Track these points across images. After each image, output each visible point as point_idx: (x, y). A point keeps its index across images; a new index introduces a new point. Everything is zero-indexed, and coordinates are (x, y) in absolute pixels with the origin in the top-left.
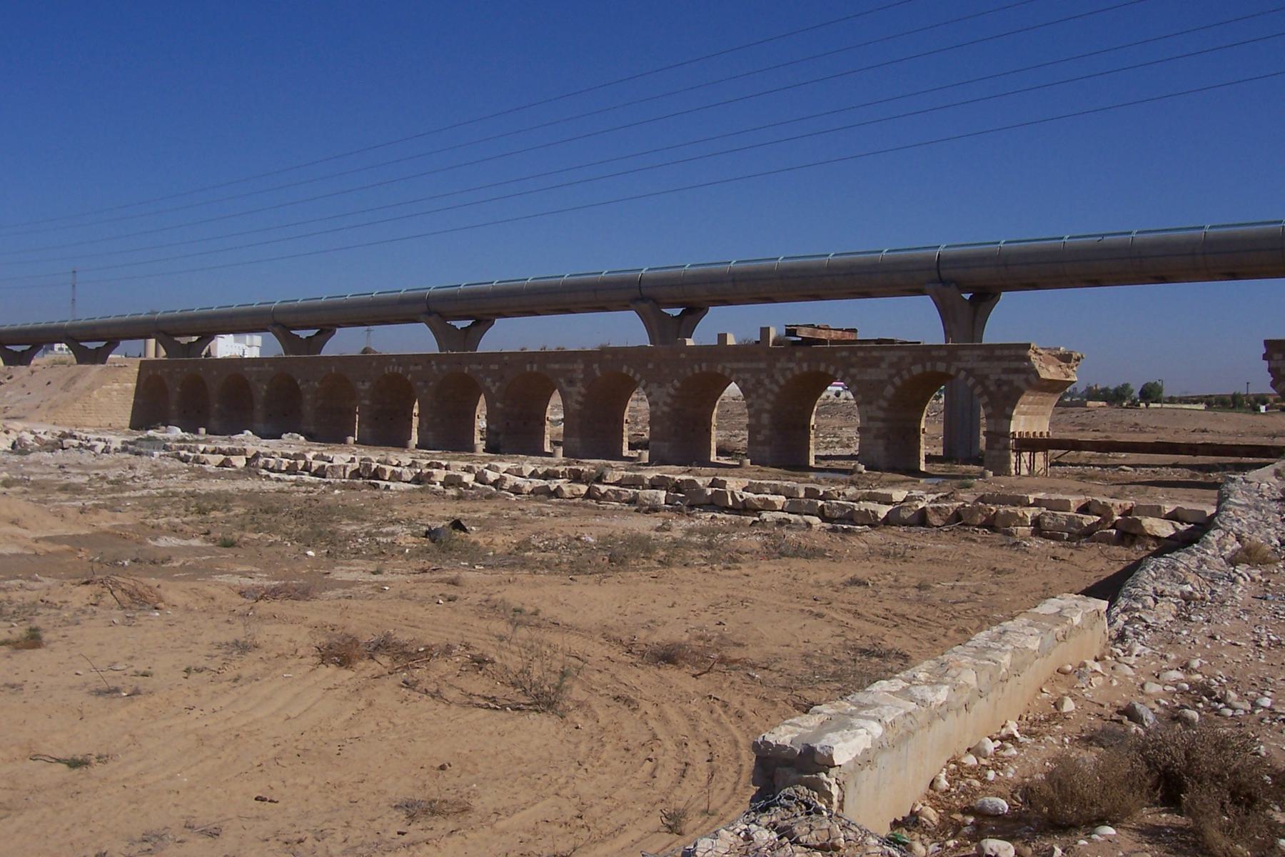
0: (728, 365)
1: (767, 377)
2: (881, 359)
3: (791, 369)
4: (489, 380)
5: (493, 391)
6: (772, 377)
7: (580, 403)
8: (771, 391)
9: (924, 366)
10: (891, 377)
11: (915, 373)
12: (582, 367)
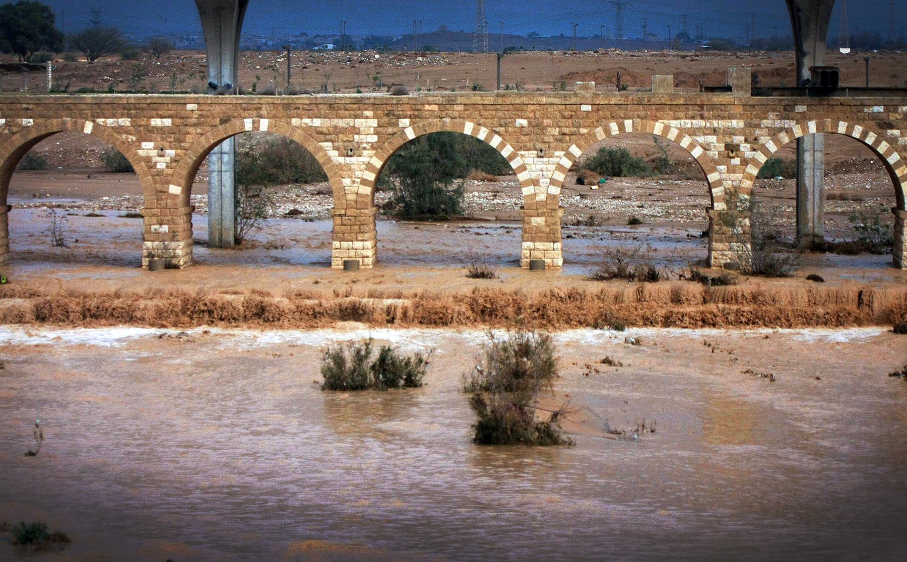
0: (674, 123)
1: (746, 141)
4: (148, 145)
5: (161, 165)
6: (754, 142)
8: (754, 161)
12: (374, 123)
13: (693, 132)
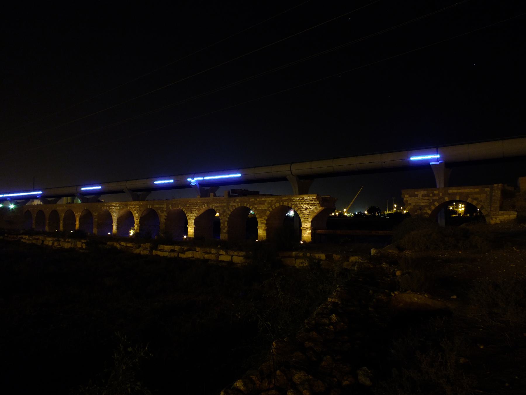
2: (265, 201)
3: (235, 206)
4: (135, 211)
7: (165, 219)
8: (228, 214)
9: (280, 204)
10: (269, 207)
11: (277, 206)
12: (166, 206)
13: (217, 207)
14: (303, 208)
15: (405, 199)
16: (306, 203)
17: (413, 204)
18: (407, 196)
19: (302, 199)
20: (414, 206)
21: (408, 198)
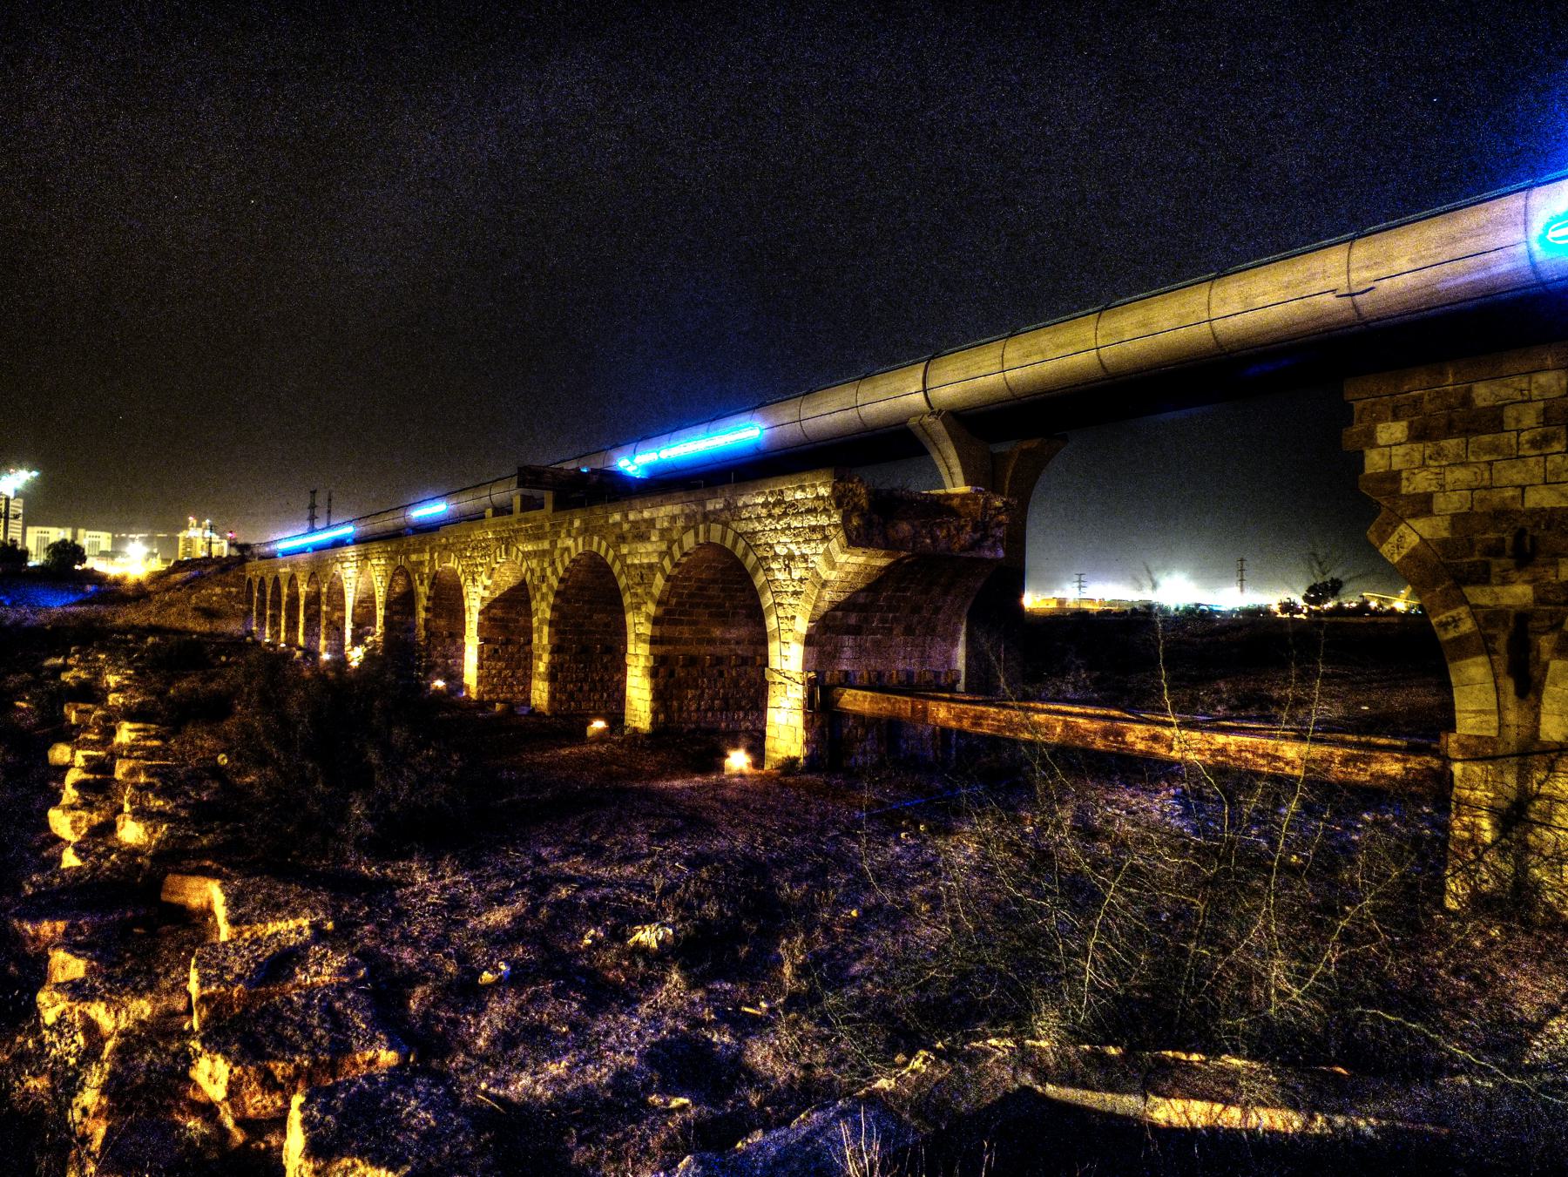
14: (776, 556)
15: (1375, 462)
16: (789, 528)
17: (1450, 503)
18: (1392, 432)
19: (775, 505)
20: (1458, 520)
21: (1401, 450)
